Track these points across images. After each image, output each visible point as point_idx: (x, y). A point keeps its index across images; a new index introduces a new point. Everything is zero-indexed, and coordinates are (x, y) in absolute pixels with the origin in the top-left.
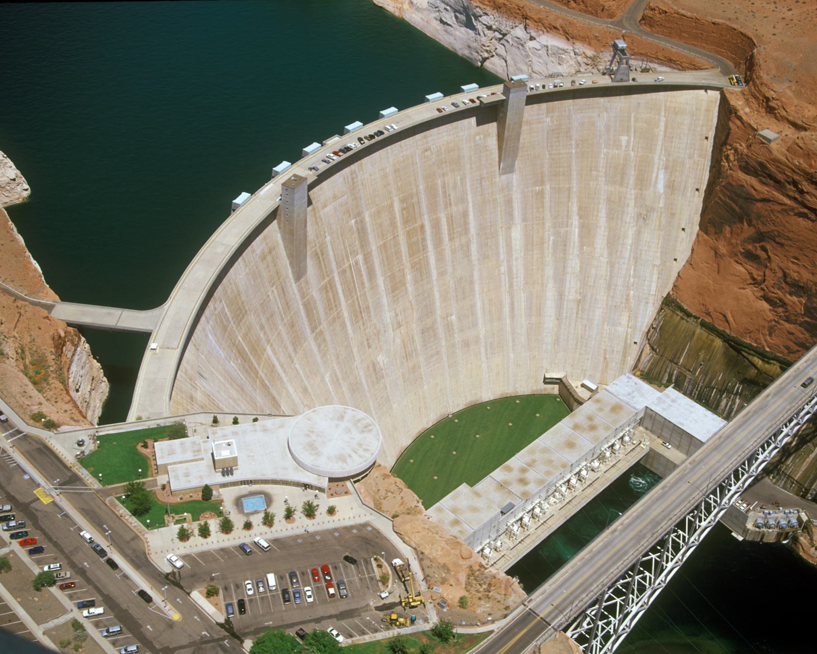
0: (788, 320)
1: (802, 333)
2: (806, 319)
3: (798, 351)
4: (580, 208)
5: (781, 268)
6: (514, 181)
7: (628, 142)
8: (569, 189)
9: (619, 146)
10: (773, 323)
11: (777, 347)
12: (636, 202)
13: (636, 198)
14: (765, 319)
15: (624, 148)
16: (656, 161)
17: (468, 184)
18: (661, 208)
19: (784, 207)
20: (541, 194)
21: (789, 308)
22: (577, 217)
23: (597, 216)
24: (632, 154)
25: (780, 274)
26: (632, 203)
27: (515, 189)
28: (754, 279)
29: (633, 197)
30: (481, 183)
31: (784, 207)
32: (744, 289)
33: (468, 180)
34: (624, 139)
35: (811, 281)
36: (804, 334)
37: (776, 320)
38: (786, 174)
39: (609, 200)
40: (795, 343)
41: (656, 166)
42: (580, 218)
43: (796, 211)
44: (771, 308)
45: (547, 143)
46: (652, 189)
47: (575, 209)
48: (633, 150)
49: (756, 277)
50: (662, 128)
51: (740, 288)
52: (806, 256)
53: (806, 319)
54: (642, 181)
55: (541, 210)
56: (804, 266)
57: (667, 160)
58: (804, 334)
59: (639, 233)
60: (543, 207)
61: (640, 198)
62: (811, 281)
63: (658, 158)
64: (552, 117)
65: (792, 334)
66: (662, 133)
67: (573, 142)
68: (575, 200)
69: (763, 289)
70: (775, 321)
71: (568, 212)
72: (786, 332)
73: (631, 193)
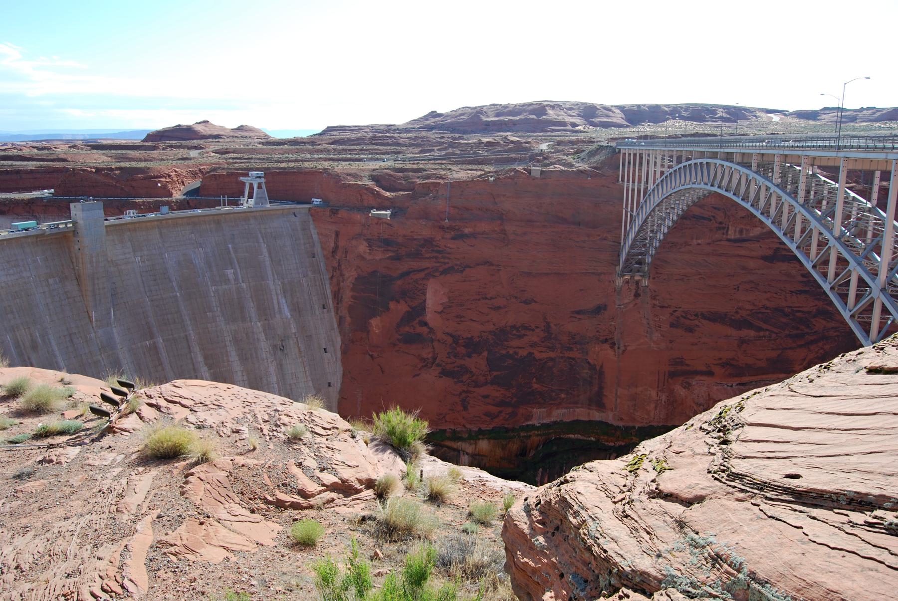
0: (477, 385)
1: (497, 391)
2: (495, 373)
3: (500, 412)
4: (206, 358)
5: (448, 334)
6: (116, 335)
7: (235, 274)
8: (187, 338)
9: (227, 281)
10: (464, 395)
11: (477, 418)
12: (266, 335)
13: (264, 330)
14: (454, 395)
15: (233, 282)
16: (272, 287)
17: (53, 343)
18: (295, 334)
19: (426, 272)
20: (155, 348)
21: (474, 370)
22: (206, 368)
23: (228, 361)
24: (244, 286)
25: (450, 340)
26: (262, 337)
27: (119, 346)
28: (423, 360)
29: (261, 329)
30: (71, 341)
31: (426, 272)
32: (418, 375)
33: (51, 337)
34: (230, 272)
35: (484, 332)
36: (499, 391)
37: (465, 389)
38: (415, 239)
39: (236, 341)
40: (494, 405)
41: (274, 293)
42: (210, 368)
43: (441, 269)
44: (455, 380)
45: (144, 287)
46: (278, 316)
47: (200, 358)
48: (243, 282)
49: (425, 356)
50: (267, 254)
51: (414, 377)
52: (469, 309)
53: (495, 373)
54: (265, 311)
55: (160, 368)
56: (471, 320)
57: (283, 283)
58: (499, 391)
59: (280, 367)
60: (161, 364)
61: (268, 329)
62: (484, 332)
63: (274, 285)
64: (141, 257)
65: (487, 397)
66: (267, 259)
67: (174, 284)
68: (197, 349)
69: (438, 365)
70: (464, 391)
71: (193, 365)
72: (480, 398)
73: (258, 326)
